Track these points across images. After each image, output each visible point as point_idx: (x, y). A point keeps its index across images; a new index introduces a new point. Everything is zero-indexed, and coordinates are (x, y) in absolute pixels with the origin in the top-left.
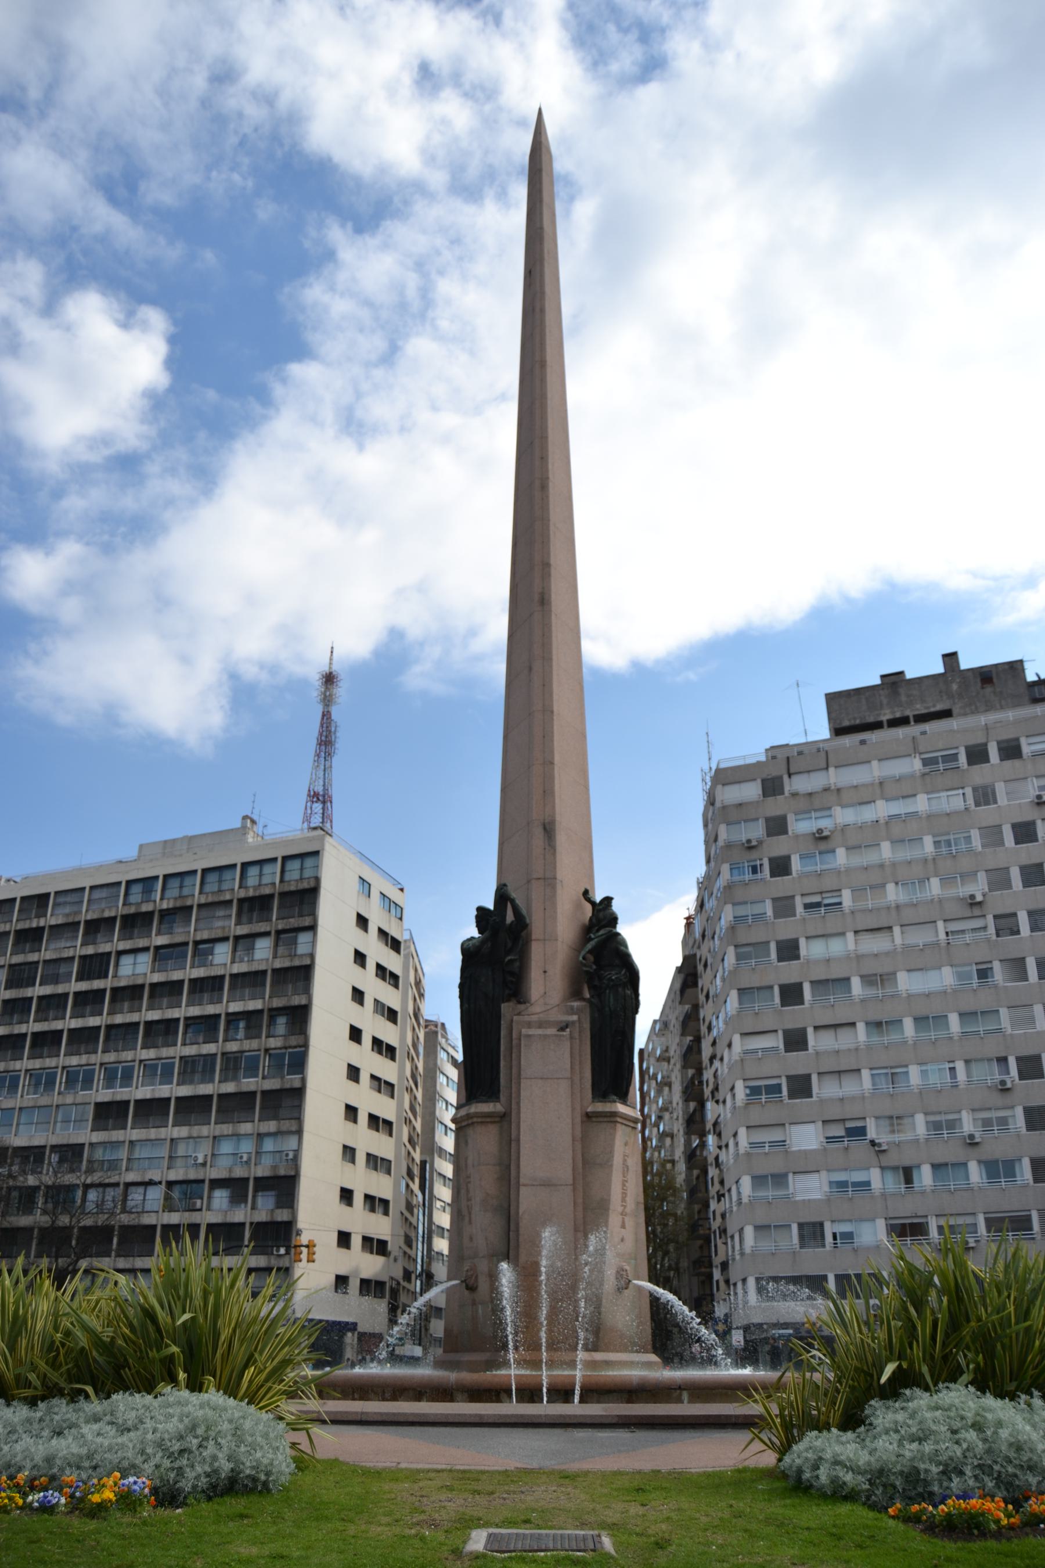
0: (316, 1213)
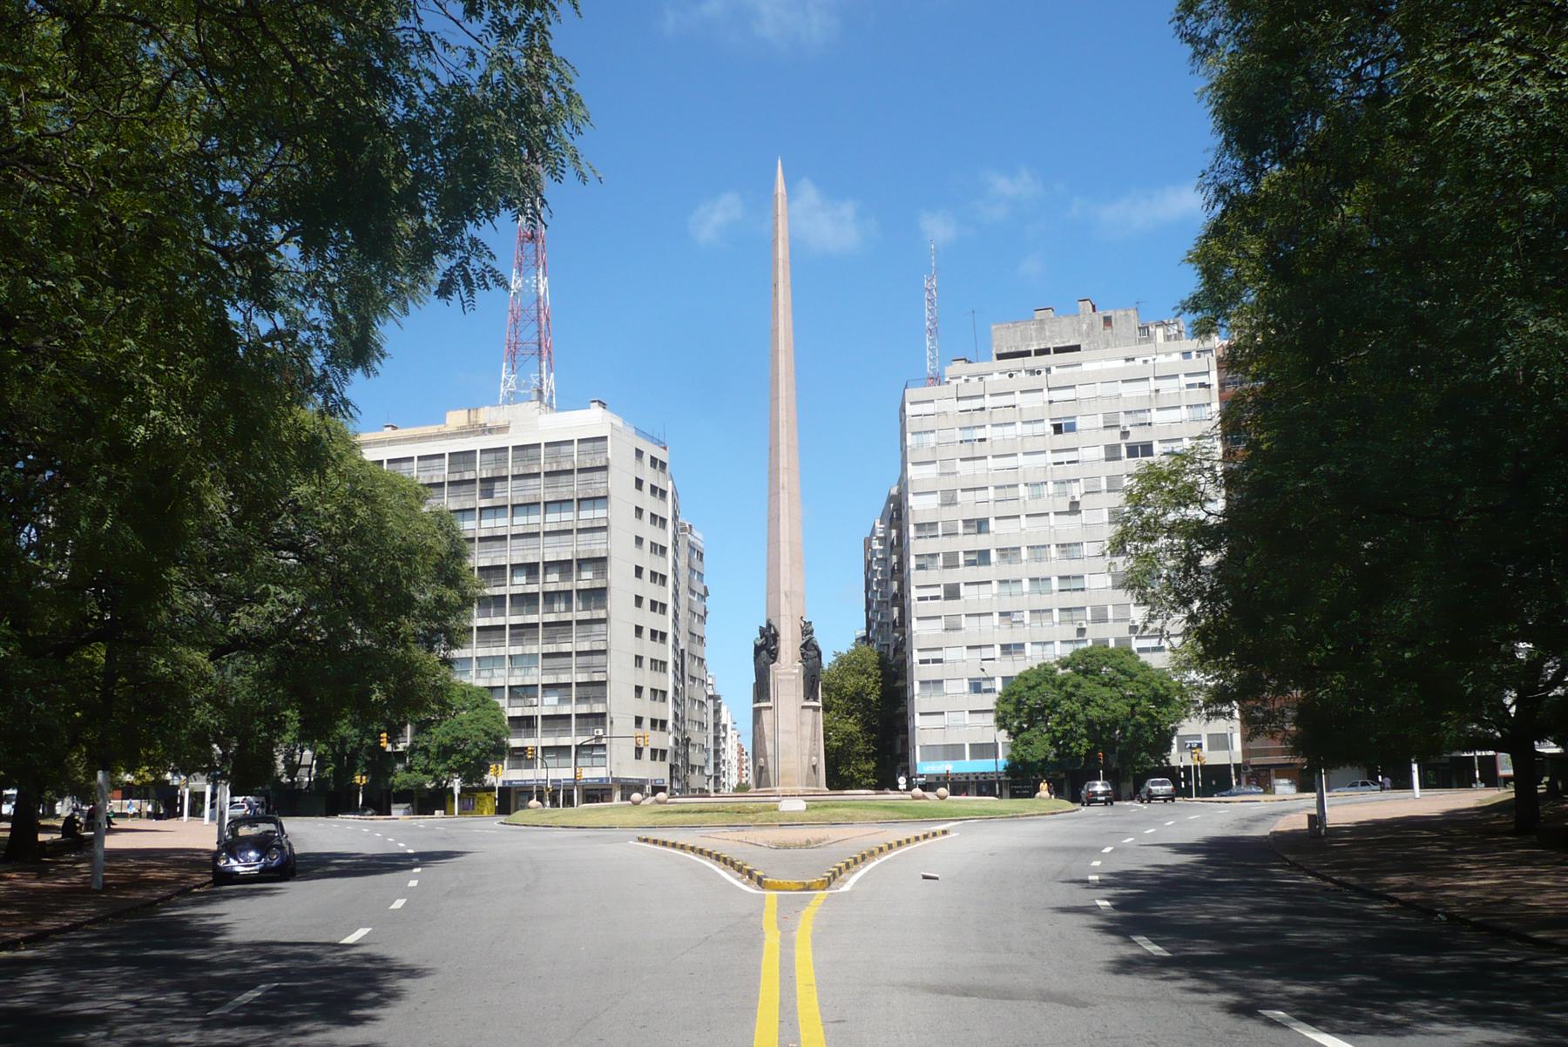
0: (620, 704)
